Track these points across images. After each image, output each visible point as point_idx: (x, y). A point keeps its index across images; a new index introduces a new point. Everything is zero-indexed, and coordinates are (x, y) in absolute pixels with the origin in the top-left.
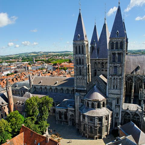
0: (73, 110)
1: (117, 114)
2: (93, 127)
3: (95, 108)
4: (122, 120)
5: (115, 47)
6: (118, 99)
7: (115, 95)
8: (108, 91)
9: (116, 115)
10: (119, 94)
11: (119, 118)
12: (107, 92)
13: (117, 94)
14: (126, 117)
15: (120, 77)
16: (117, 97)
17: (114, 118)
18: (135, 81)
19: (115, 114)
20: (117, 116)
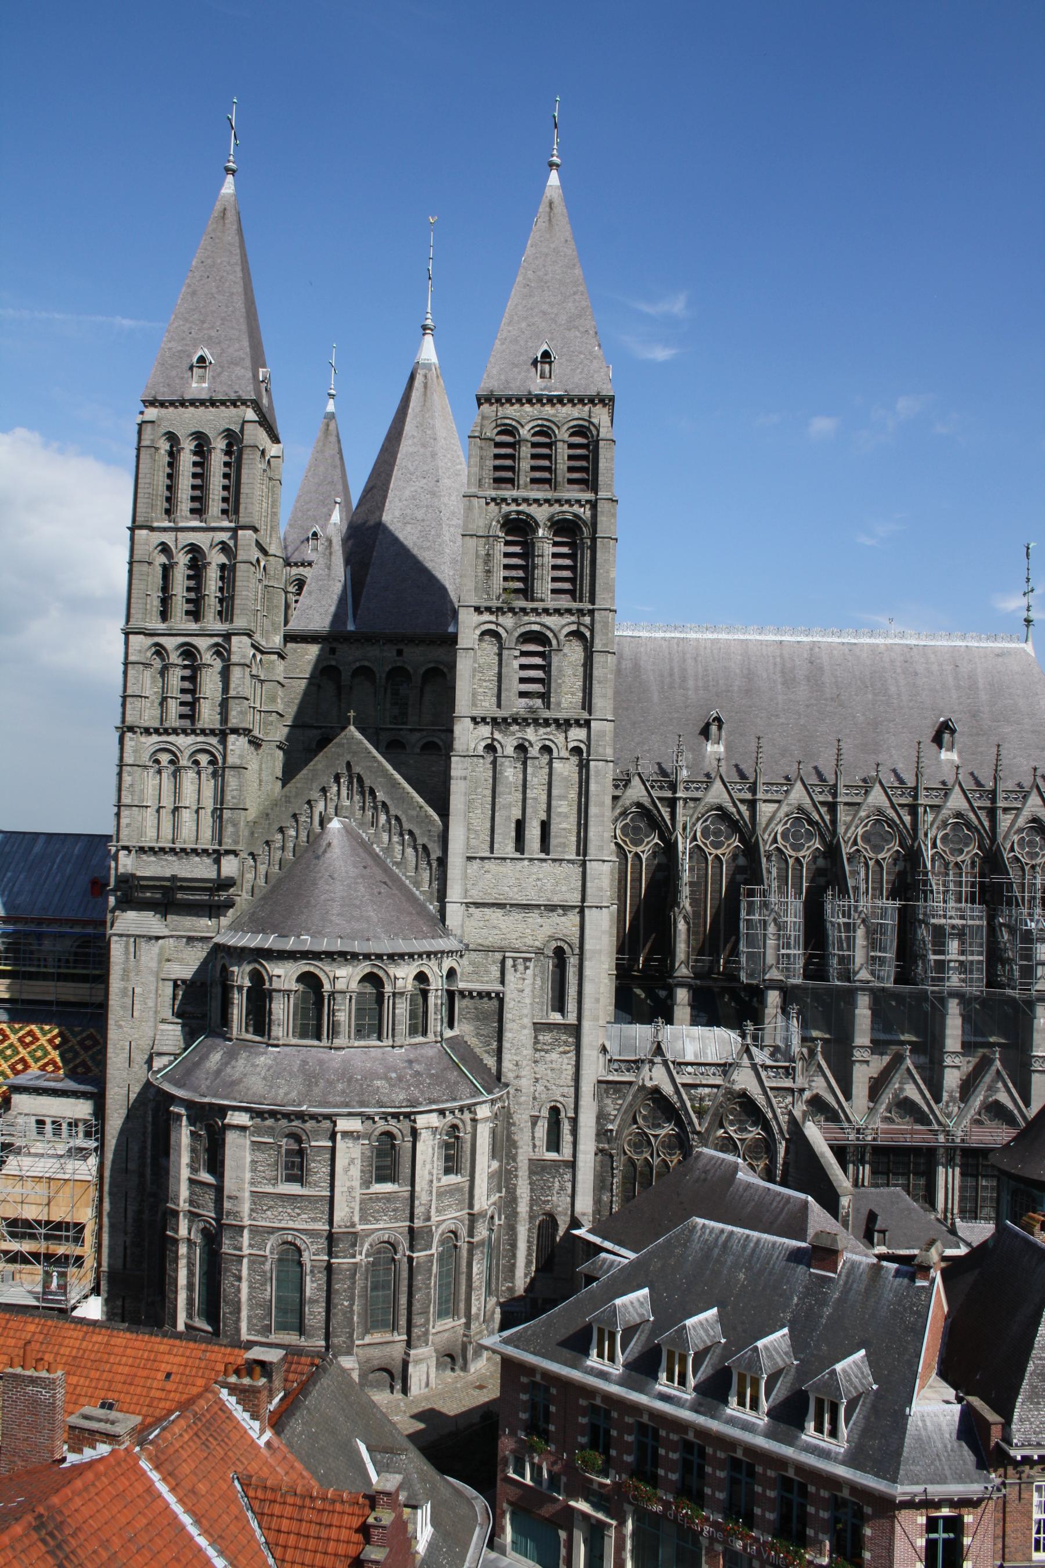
0: (73, 1124)
1: (555, 1111)
2: (306, 1257)
3: (334, 1032)
4: (601, 1184)
5: (525, 465)
6: (559, 952)
7: (534, 917)
8: (465, 876)
9: (542, 1130)
10: (566, 908)
11: (572, 1165)
12: (454, 893)
13: (552, 908)
14: (642, 1141)
15: (577, 734)
16: (547, 930)
17: (523, 1172)
18: (694, 839)
19: (535, 1120)
20: (554, 1144)
